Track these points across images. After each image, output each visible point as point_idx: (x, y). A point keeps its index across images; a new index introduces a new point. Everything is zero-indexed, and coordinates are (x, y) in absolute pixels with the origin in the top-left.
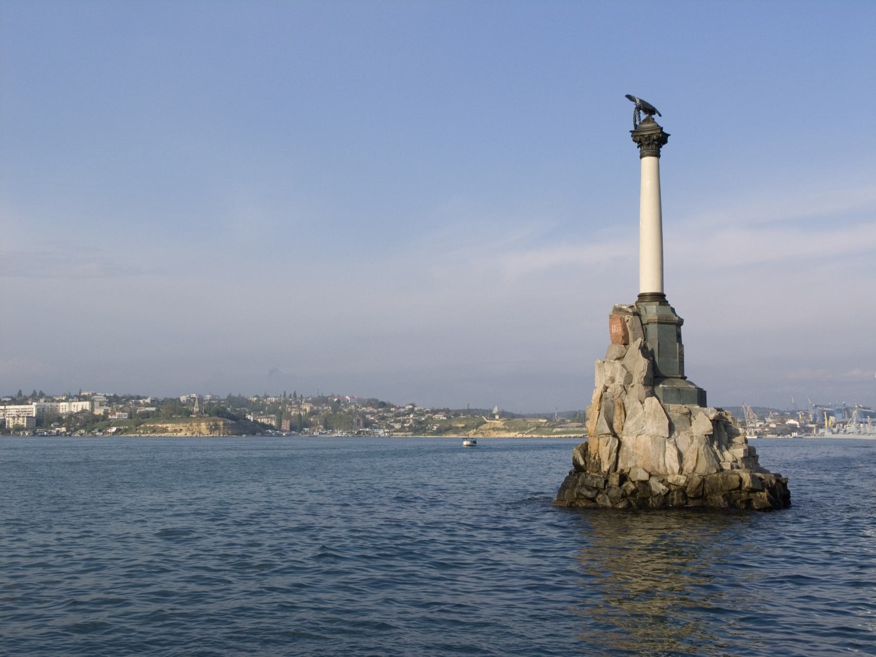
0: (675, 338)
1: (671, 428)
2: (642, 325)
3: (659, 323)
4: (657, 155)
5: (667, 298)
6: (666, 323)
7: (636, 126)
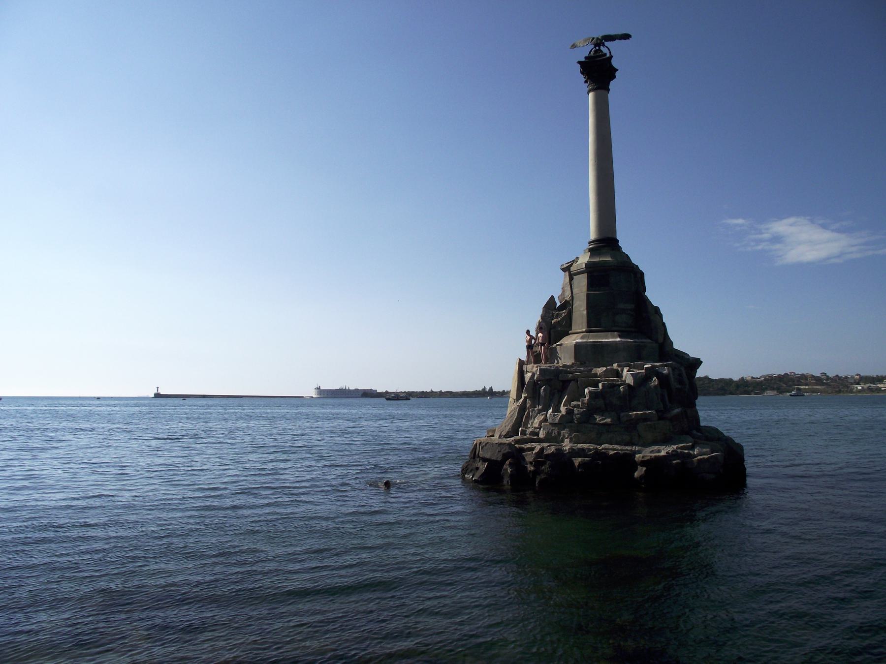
0: (585, 289)
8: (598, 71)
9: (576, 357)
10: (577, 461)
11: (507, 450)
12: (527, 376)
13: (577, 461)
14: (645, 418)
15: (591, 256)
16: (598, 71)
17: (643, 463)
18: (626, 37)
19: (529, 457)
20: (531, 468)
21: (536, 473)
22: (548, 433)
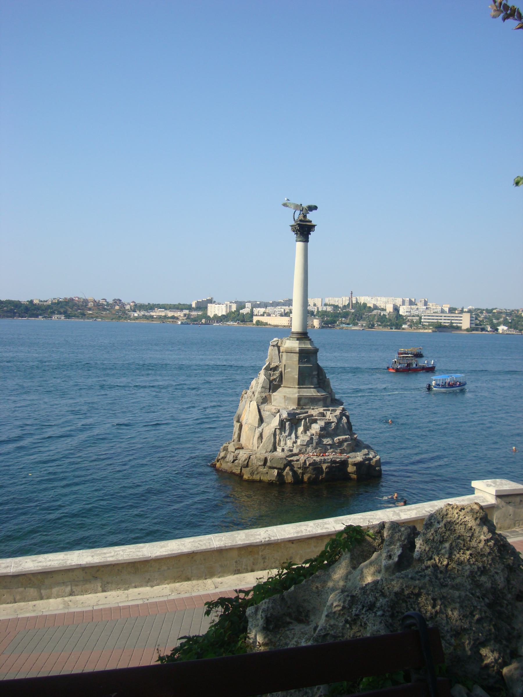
0: (297, 363)
1: (261, 420)
2: (279, 352)
3: (287, 352)
4: (306, 240)
5: (309, 335)
6: (291, 353)
7: (294, 220)
8: (304, 230)
9: (299, 404)
10: (324, 466)
11: (286, 462)
12: (265, 414)
13: (324, 466)
14: (346, 440)
15: (299, 343)
16: (304, 230)
17: (355, 464)
18: (315, 208)
19: (296, 465)
20: (300, 471)
21: (303, 474)
22: (300, 451)
